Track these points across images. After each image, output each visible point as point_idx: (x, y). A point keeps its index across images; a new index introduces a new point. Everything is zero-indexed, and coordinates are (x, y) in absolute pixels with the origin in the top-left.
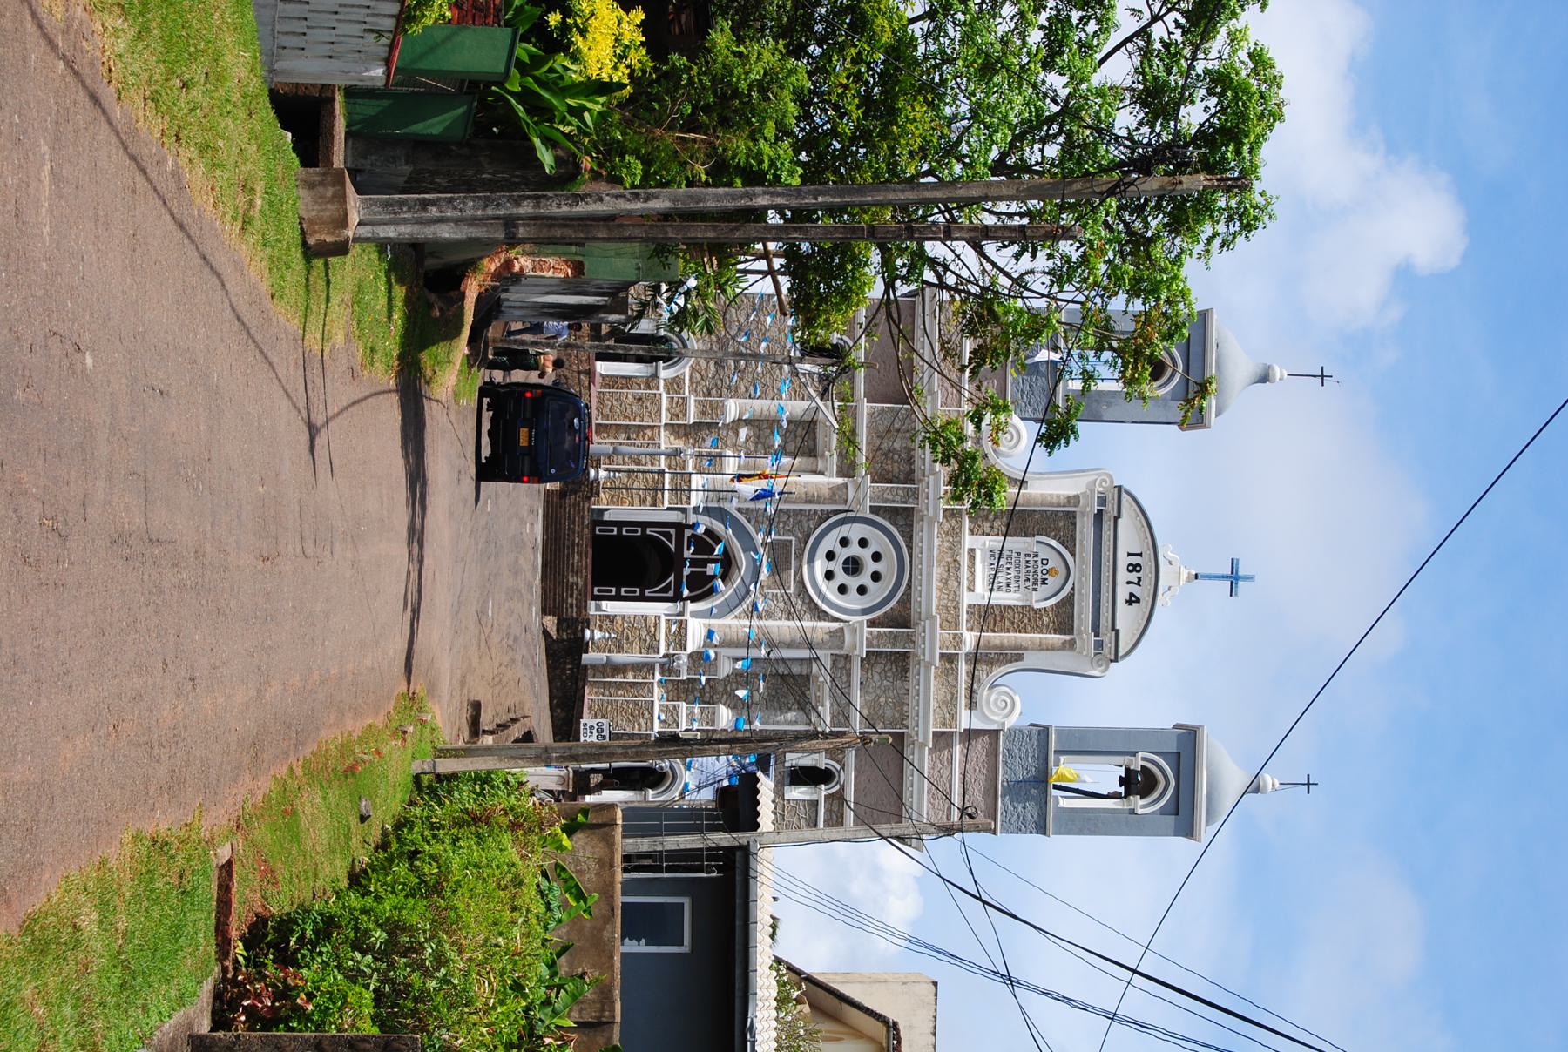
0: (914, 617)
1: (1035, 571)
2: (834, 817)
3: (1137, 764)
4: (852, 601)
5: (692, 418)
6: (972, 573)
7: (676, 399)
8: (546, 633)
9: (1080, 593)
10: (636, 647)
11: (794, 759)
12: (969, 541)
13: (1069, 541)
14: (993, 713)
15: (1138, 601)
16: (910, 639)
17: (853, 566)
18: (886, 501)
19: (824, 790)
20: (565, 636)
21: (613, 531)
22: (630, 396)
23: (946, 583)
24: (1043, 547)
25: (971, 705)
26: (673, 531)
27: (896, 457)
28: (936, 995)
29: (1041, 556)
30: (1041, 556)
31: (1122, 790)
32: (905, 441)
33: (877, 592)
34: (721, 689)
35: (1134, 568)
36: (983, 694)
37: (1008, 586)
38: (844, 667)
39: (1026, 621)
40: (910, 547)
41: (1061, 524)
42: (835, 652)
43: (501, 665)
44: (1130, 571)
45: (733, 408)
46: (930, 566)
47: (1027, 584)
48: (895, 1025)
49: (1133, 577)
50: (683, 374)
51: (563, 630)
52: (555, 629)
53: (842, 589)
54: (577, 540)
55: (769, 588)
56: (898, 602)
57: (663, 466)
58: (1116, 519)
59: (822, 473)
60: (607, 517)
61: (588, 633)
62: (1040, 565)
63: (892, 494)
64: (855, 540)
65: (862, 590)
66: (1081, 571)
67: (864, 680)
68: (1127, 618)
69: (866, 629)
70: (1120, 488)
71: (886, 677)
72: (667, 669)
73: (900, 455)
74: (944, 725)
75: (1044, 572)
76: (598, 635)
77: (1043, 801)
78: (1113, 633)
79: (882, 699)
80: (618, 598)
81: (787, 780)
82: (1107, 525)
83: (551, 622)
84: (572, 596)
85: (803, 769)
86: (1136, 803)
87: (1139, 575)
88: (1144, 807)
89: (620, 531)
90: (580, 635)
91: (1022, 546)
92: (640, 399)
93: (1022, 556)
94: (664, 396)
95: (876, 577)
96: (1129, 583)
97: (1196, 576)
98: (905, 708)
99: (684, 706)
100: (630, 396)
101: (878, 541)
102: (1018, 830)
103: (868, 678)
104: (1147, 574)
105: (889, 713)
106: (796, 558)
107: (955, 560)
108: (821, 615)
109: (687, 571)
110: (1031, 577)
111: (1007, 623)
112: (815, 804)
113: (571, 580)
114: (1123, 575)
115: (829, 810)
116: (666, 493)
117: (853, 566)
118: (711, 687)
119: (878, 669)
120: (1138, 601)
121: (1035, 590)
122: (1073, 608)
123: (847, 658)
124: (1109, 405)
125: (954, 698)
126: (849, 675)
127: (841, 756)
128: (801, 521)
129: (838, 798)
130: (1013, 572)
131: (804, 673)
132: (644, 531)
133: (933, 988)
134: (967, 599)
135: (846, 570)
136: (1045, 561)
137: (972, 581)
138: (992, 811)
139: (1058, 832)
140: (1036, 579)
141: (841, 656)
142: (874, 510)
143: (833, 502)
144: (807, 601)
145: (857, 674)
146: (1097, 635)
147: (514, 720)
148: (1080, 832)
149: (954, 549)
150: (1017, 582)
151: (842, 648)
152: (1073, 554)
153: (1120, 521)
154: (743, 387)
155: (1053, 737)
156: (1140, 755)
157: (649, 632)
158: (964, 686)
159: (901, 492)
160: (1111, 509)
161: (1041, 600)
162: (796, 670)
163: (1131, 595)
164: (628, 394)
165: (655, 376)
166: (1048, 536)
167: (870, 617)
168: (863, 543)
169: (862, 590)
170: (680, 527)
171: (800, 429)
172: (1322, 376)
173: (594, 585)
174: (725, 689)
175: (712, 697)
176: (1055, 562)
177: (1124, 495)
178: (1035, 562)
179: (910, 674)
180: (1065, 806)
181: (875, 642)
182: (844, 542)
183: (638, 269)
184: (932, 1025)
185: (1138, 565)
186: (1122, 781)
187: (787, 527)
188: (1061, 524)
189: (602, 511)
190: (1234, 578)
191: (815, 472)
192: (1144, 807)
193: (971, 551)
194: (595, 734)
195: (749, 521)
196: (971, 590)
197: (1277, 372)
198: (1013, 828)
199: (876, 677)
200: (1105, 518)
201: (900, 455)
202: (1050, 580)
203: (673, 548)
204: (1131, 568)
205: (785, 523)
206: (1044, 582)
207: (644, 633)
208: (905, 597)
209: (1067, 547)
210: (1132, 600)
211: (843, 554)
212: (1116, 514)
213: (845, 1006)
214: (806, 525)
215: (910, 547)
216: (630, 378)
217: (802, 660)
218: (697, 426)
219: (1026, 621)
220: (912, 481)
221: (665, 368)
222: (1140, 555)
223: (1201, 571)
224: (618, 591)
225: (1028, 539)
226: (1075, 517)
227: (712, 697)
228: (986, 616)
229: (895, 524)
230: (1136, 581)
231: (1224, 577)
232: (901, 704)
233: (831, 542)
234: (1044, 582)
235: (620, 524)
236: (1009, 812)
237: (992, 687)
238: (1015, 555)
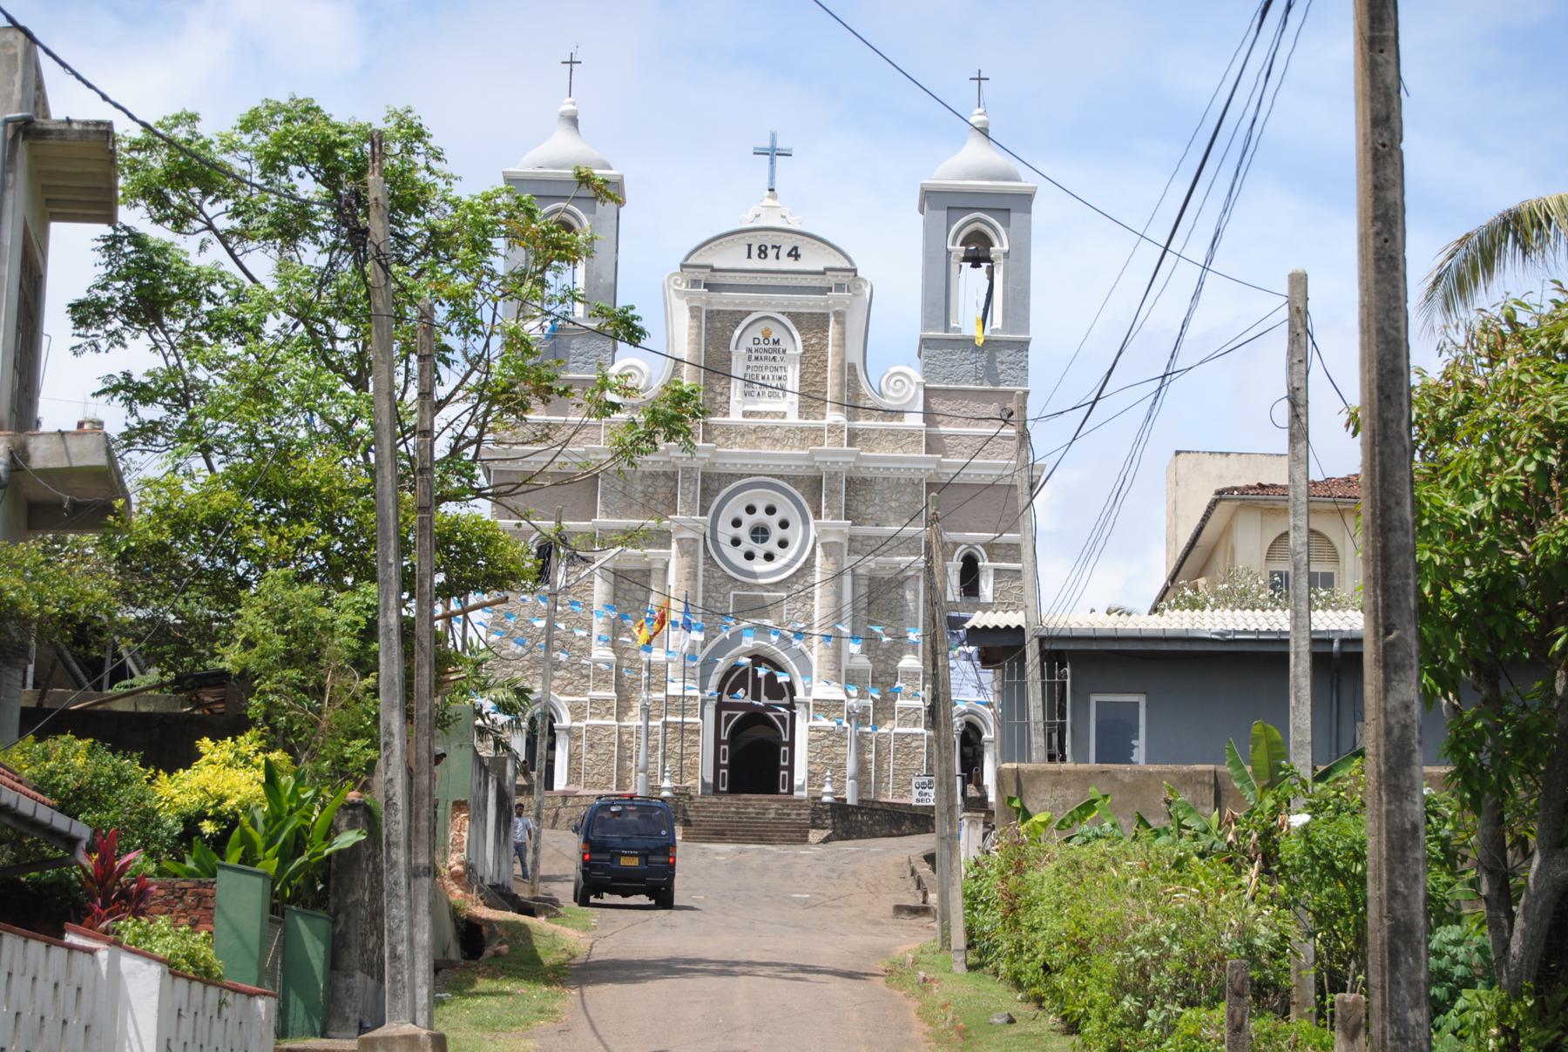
0: (811, 472)
1: (765, 351)
3: (959, 250)
4: (795, 534)
5: (612, 694)
6: (767, 414)
8: (826, 840)
9: (788, 306)
10: (840, 750)
11: (953, 590)
12: (735, 417)
13: (736, 317)
14: (907, 393)
15: (795, 248)
16: (833, 477)
17: (760, 533)
18: (694, 499)
19: (984, 563)
23: (777, 440)
24: (741, 343)
25: (897, 413)
26: (724, 714)
27: (650, 490)
28: (1188, 452)
29: (750, 345)
30: (750, 345)
31: (984, 265)
33: (786, 509)
34: (882, 666)
35: (763, 252)
36: (888, 403)
39: (815, 361)
40: (741, 476)
41: (719, 325)
42: (846, 552)
43: (858, 885)
44: (766, 256)
45: (601, 653)
46: (760, 456)
47: (778, 359)
48: (1219, 493)
49: (771, 253)
50: (567, 703)
52: (821, 832)
53: (783, 544)
54: (733, 809)
55: (781, 617)
57: (659, 723)
58: (713, 270)
59: (667, 564)
60: (710, 779)
61: (826, 799)
63: (688, 493)
64: (734, 532)
65: (784, 524)
67: (874, 523)
68: (813, 260)
69: (823, 521)
70: (683, 266)
71: (871, 500)
72: (860, 718)
74: (919, 442)
76: (828, 788)
80: (791, 768)
81: (974, 599)
82: (720, 279)
83: (815, 835)
84: (789, 815)
85: (962, 581)
86: (998, 251)
88: (1001, 244)
89: (724, 767)
90: (827, 807)
91: (740, 363)
92: (592, 746)
93: (750, 364)
94: (589, 721)
96: (777, 257)
97: (771, 190)
98: (902, 481)
99: (899, 703)
101: (735, 508)
102: (1025, 369)
106: (751, 590)
107: (755, 431)
108: (809, 564)
111: (817, 379)
113: (773, 815)
114: (770, 263)
116: (686, 720)
117: (760, 533)
120: (795, 248)
121: (784, 351)
123: (852, 539)
124: (599, 276)
125: (893, 433)
126: (869, 538)
127: (950, 546)
128: (715, 585)
129: (991, 548)
130: (767, 373)
131: (867, 582)
132: (724, 742)
133: (1182, 455)
134: (793, 419)
135: (764, 540)
136: (756, 341)
137: (776, 414)
139: (1027, 330)
140: (774, 350)
141: (850, 546)
142: (704, 512)
143: (696, 551)
145: (867, 530)
146: (830, 289)
147: (913, 872)
148: (1026, 306)
149: (743, 432)
150: (776, 369)
151: (842, 544)
152: (749, 313)
153: (717, 265)
156: (950, 247)
157: (825, 737)
158: (880, 423)
159: (686, 485)
160: (704, 275)
161: (795, 345)
162: (863, 590)
163: (789, 255)
164: (586, 757)
165: (569, 731)
166: (730, 339)
167: (811, 516)
168: (737, 523)
169: (784, 524)
170: (720, 707)
171: (623, 586)
172: (571, 62)
173: (776, 792)
174: (882, 661)
175: (891, 675)
176: (757, 332)
177: (690, 262)
179: (868, 476)
181: (836, 511)
182: (736, 542)
183: (461, 746)
184: (1218, 456)
185: (760, 248)
186: (976, 265)
189: (704, 785)
190: (773, 153)
191: (666, 571)
192: (1001, 244)
193: (745, 414)
194: (927, 790)
195: (714, 637)
196: (784, 415)
197: (567, 107)
198: (1022, 374)
199: (871, 510)
200: (713, 281)
202: (774, 336)
203: (740, 713)
205: (716, 601)
206: (776, 342)
207: (827, 743)
209: (742, 319)
210: (794, 254)
211: (748, 544)
213: (1200, 542)
215: (741, 476)
216: (570, 756)
217: (853, 584)
218: (619, 687)
219: (815, 361)
220: (675, 473)
222: (750, 246)
223: (766, 185)
224: (785, 768)
225: (734, 358)
226: (712, 311)
227: (891, 675)
228: (811, 398)
229: (718, 491)
230: (775, 250)
231: (772, 162)
232: (898, 486)
233: (736, 556)
234: (776, 342)
235: (717, 766)
237: (881, 394)
238: (749, 371)
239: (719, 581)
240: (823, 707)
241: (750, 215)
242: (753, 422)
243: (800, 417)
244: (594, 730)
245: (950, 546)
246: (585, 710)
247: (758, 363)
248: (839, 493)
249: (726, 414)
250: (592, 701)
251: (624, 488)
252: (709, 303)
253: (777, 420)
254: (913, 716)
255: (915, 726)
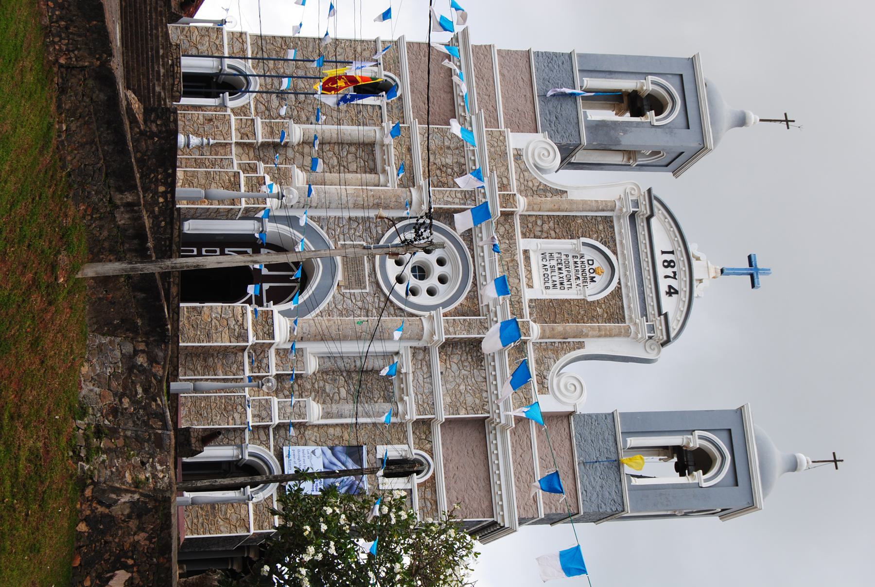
2: (429, 504)
6: (530, 271)
7: (244, 121)
9: (627, 285)
10: (226, 336)
12: (523, 243)
13: (610, 242)
15: (676, 292)
18: (447, 203)
19: (416, 479)
20: (154, 129)
21: (193, 251)
22: (201, 117)
25: (543, 388)
27: (449, 170)
32: (455, 157)
33: (444, 292)
35: (669, 264)
36: (552, 379)
37: (561, 284)
38: (424, 359)
40: (472, 249)
41: (601, 227)
44: (666, 267)
45: (296, 133)
47: (578, 282)
49: (669, 271)
51: (152, 122)
55: (346, 288)
56: (466, 298)
61: (181, 139)
62: (586, 265)
66: (624, 264)
67: (444, 370)
69: (442, 318)
73: (452, 169)
75: (591, 271)
76: (195, 141)
77: (618, 480)
78: (662, 317)
79: (462, 387)
86: (700, 478)
87: (674, 269)
88: (706, 481)
91: (570, 247)
92: (210, 120)
93: (570, 258)
94: (233, 118)
95: (442, 280)
96: (666, 277)
98: (484, 395)
100: (201, 117)
103: (446, 368)
104: (681, 267)
105: (469, 399)
107: (513, 260)
109: (266, 286)
110: (580, 276)
112: (410, 491)
114: (661, 271)
115: (423, 498)
118: (299, 386)
119: (455, 359)
120: (676, 292)
122: (621, 300)
123: (425, 349)
124: (625, 132)
126: (429, 366)
130: (565, 273)
134: (528, 295)
136: (591, 262)
137: (530, 279)
138: (573, 491)
140: (585, 278)
141: (419, 349)
144: (382, 299)
145: (437, 365)
152: (615, 253)
153: (653, 221)
154: (304, 116)
155: (618, 420)
156: (697, 433)
159: (459, 195)
161: (594, 292)
163: (670, 287)
165: (223, 106)
169: (431, 292)
176: (599, 262)
178: (583, 262)
180: (637, 484)
181: (451, 329)
185: (672, 261)
187: (357, 234)
188: (601, 227)
192: (706, 481)
195: (322, 228)
196: (530, 286)
197: (753, 118)
199: (455, 367)
201: (452, 169)
202: (597, 278)
204: (666, 264)
205: (355, 230)
206: (592, 280)
207: (232, 323)
208: (472, 294)
209: (609, 247)
212: (649, 213)
214: (375, 232)
215: (472, 249)
218: (264, 145)
219: (582, 313)
221: (230, 100)
222: (672, 252)
223: (726, 266)
225: (574, 241)
226: (612, 221)
230: (672, 275)
234: (592, 280)
236: (588, 491)
238: (563, 257)
239: (374, 232)
240: (266, 325)
241: (697, 254)
242: (520, 258)
243: (531, 301)
244: (226, 121)
245: (428, 446)
246: (245, 115)
247: (572, 264)
248: (469, 332)
249: (524, 235)
250: (253, 120)
251: (449, 148)
252: (619, 218)
253: (524, 280)
254: (264, 414)
255: (254, 416)
